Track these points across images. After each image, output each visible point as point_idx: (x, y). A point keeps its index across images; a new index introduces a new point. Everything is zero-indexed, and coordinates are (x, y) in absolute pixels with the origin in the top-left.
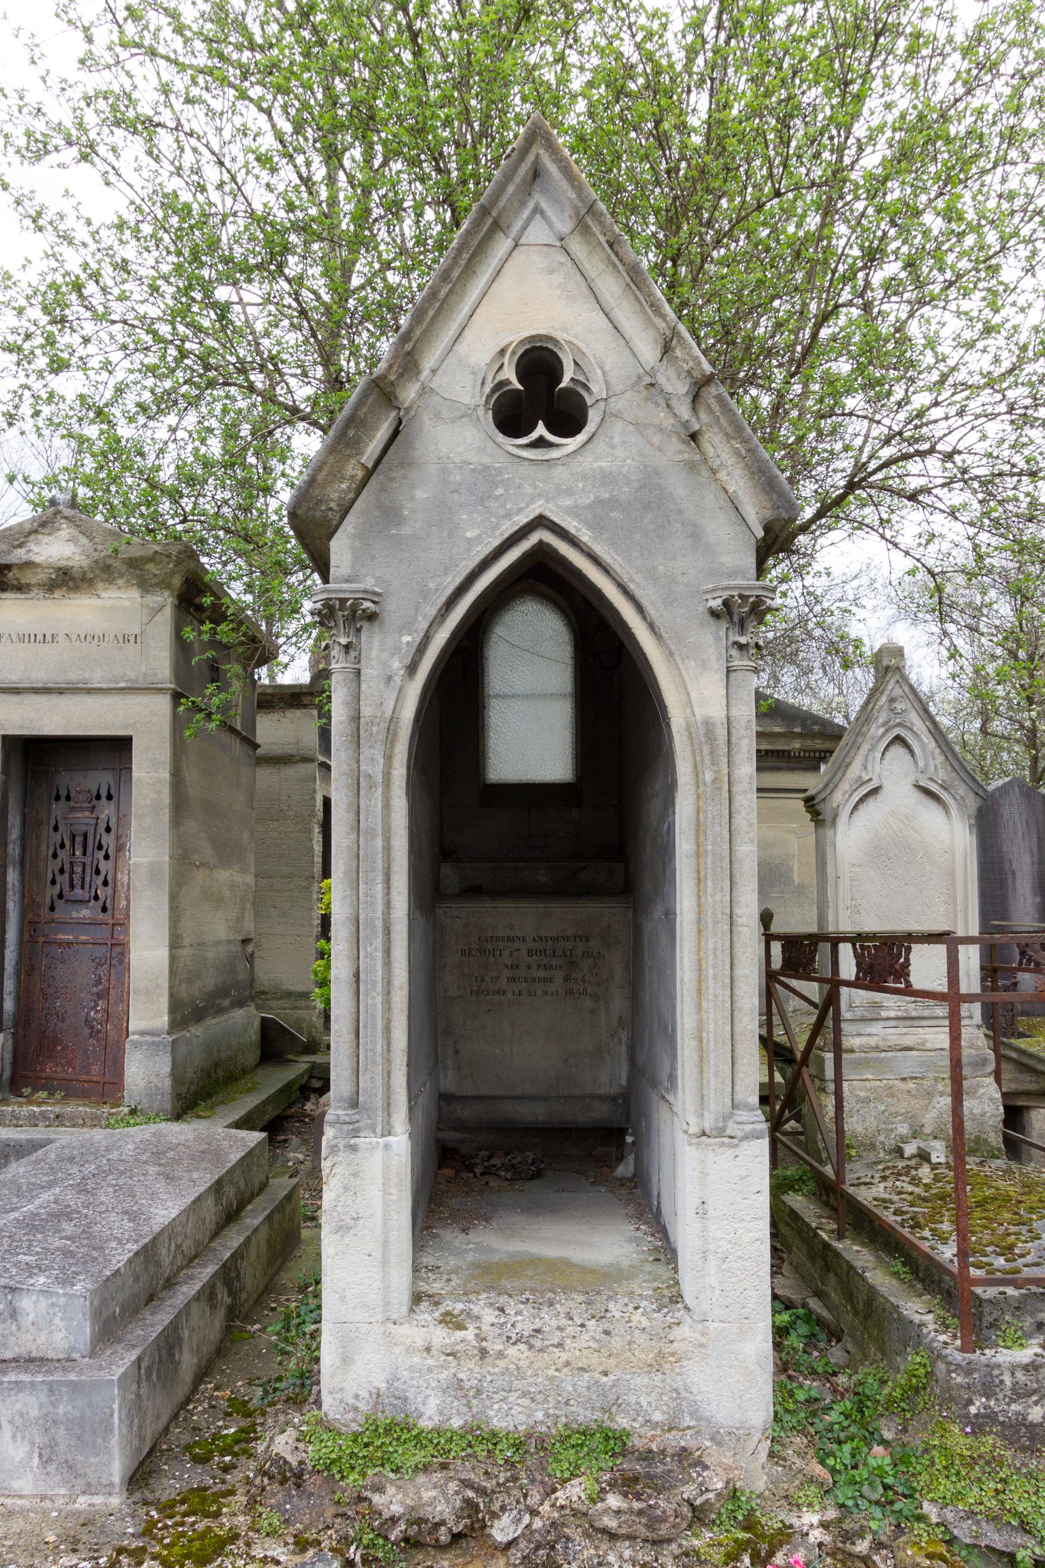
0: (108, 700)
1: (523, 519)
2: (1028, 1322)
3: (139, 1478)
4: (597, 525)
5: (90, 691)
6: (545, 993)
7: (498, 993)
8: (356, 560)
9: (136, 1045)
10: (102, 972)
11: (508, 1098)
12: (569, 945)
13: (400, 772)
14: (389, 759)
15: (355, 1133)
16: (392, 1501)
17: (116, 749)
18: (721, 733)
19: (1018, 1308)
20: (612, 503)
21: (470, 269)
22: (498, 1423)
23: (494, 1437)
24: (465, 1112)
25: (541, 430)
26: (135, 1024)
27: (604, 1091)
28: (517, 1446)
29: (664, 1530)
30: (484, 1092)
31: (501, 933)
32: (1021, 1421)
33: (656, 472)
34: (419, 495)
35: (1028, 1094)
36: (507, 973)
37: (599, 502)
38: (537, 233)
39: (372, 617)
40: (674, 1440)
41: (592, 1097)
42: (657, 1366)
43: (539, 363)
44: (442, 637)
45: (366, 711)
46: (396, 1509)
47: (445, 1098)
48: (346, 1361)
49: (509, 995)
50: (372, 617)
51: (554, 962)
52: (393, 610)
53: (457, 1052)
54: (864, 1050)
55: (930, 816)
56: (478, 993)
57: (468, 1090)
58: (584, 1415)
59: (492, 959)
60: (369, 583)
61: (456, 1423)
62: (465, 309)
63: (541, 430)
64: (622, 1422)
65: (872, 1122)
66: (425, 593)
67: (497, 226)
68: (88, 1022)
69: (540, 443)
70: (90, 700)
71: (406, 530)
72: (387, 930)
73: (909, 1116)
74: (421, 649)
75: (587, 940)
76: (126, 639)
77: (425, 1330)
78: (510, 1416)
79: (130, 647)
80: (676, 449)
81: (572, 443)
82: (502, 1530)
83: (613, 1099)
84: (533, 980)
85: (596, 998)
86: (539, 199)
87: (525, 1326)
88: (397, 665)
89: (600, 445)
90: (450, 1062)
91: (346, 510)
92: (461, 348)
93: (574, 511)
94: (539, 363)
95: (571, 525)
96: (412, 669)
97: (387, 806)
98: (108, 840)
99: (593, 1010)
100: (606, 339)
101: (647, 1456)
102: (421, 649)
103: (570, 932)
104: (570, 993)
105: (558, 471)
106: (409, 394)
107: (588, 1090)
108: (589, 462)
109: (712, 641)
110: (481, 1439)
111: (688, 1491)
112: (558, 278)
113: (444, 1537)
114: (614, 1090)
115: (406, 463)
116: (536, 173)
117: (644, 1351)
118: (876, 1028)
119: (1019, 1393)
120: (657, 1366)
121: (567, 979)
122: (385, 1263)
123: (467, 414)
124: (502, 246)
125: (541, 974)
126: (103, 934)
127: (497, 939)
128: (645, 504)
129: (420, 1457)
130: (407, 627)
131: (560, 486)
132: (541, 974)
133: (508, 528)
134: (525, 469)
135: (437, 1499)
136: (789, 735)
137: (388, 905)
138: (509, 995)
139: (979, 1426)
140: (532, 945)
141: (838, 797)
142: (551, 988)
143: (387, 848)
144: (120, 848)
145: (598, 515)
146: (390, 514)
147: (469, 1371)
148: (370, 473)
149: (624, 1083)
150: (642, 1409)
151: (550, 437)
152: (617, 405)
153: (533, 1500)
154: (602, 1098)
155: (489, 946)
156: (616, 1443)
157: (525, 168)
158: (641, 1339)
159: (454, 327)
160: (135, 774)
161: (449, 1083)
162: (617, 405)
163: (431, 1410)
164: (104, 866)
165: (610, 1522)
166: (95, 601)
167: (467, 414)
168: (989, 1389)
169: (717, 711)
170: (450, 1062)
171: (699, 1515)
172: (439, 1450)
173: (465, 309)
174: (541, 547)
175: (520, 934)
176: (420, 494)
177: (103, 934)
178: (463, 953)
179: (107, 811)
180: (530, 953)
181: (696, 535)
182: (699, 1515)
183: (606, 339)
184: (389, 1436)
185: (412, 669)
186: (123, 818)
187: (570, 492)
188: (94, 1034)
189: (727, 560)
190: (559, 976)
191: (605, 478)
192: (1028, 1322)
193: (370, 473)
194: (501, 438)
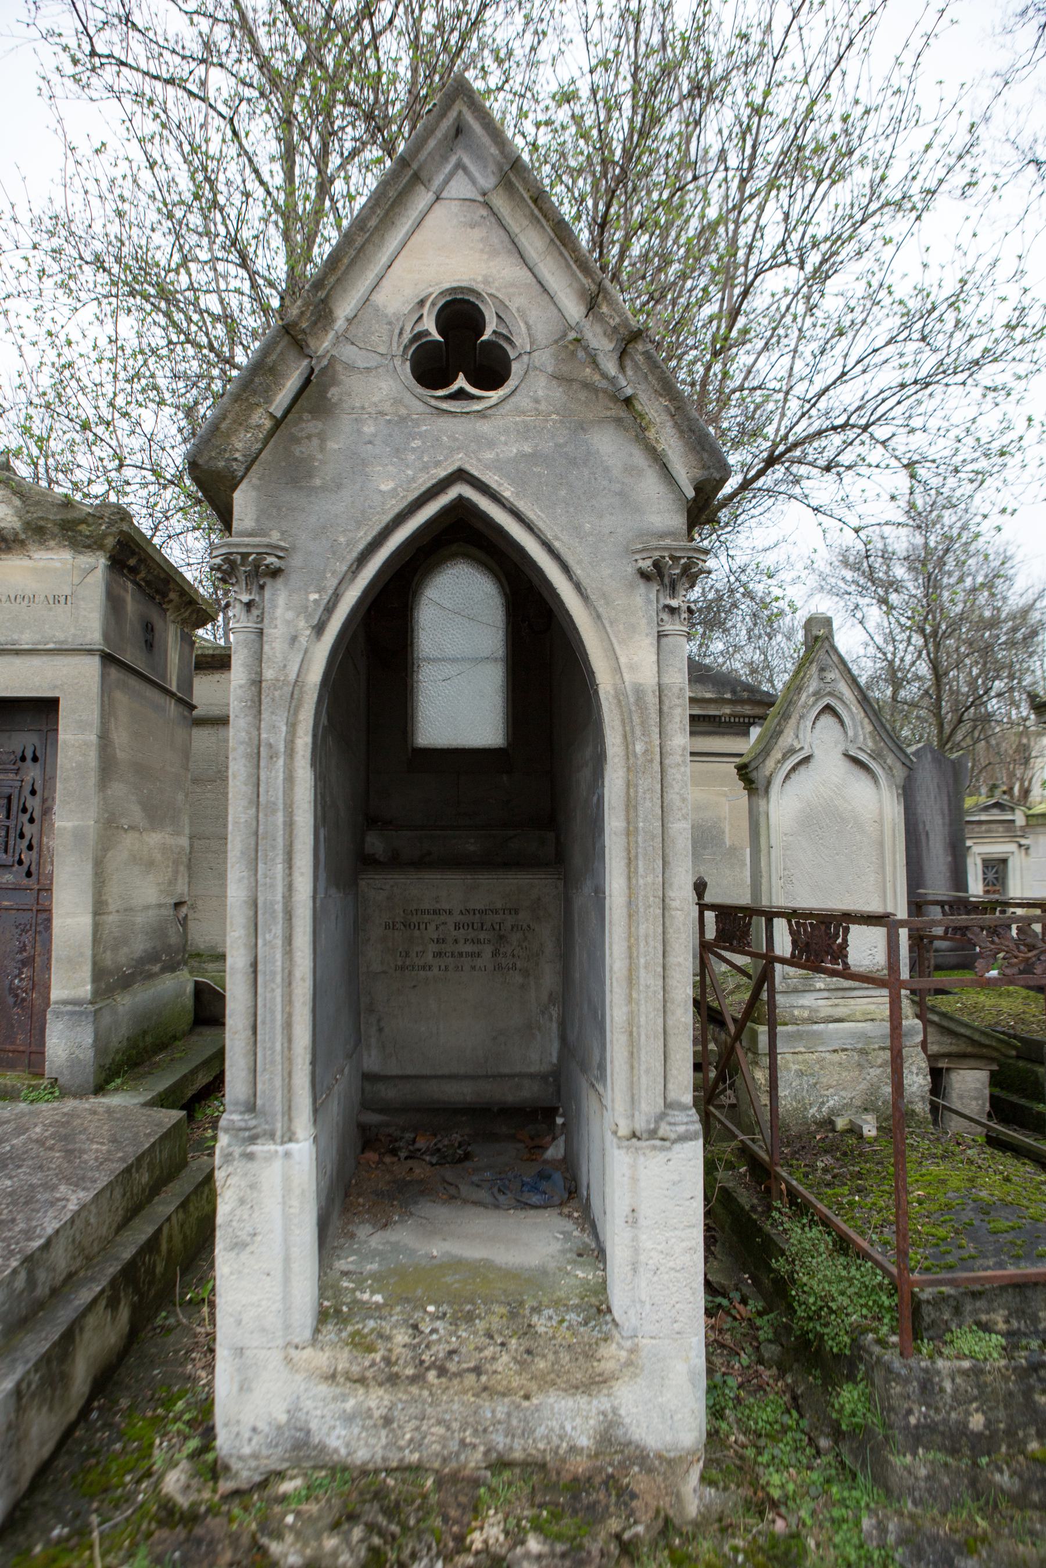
1: (442, 473)
6: (473, 968)
7: (424, 968)
8: (263, 513)
11: (436, 1077)
12: (497, 918)
13: (304, 741)
14: (292, 727)
18: (652, 700)
24: (389, 1093)
25: (461, 382)
26: (56, 994)
27: (533, 1069)
30: (410, 1071)
31: (426, 906)
36: (432, 948)
38: (459, 187)
39: (275, 573)
41: (521, 1075)
43: (460, 314)
45: (269, 674)
47: (369, 1078)
49: (436, 970)
51: (482, 936)
53: (380, 1030)
56: (402, 968)
57: (393, 1069)
59: (417, 933)
60: (275, 537)
62: (383, 259)
63: (461, 382)
67: (417, 179)
69: (460, 395)
75: (516, 912)
81: (495, 395)
83: (543, 1077)
84: (461, 954)
85: (526, 973)
90: (373, 1040)
93: (497, 466)
94: (460, 314)
95: (491, 479)
97: (290, 779)
99: (522, 986)
102: (330, 609)
103: (499, 905)
104: (498, 968)
107: (517, 1069)
114: (545, 1068)
116: (459, 130)
121: (495, 953)
124: (422, 198)
125: (468, 948)
127: (423, 912)
132: (468, 948)
133: (425, 482)
137: (290, 887)
138: (436, 970)
140: (458, 918)
142: (479, 962)
143: (290, 825)
149: (555, 1060)
154: (532, 1076)
155: (415, 919)
157: (447, 123)
161: (372, 1062)
170: (373, 1040)
173: (383, 259)
174: (461, 502)
175: (446, 906)
178: (387, 926)
180: (457, 926)
185: (319, 629)
190: (488, 950)
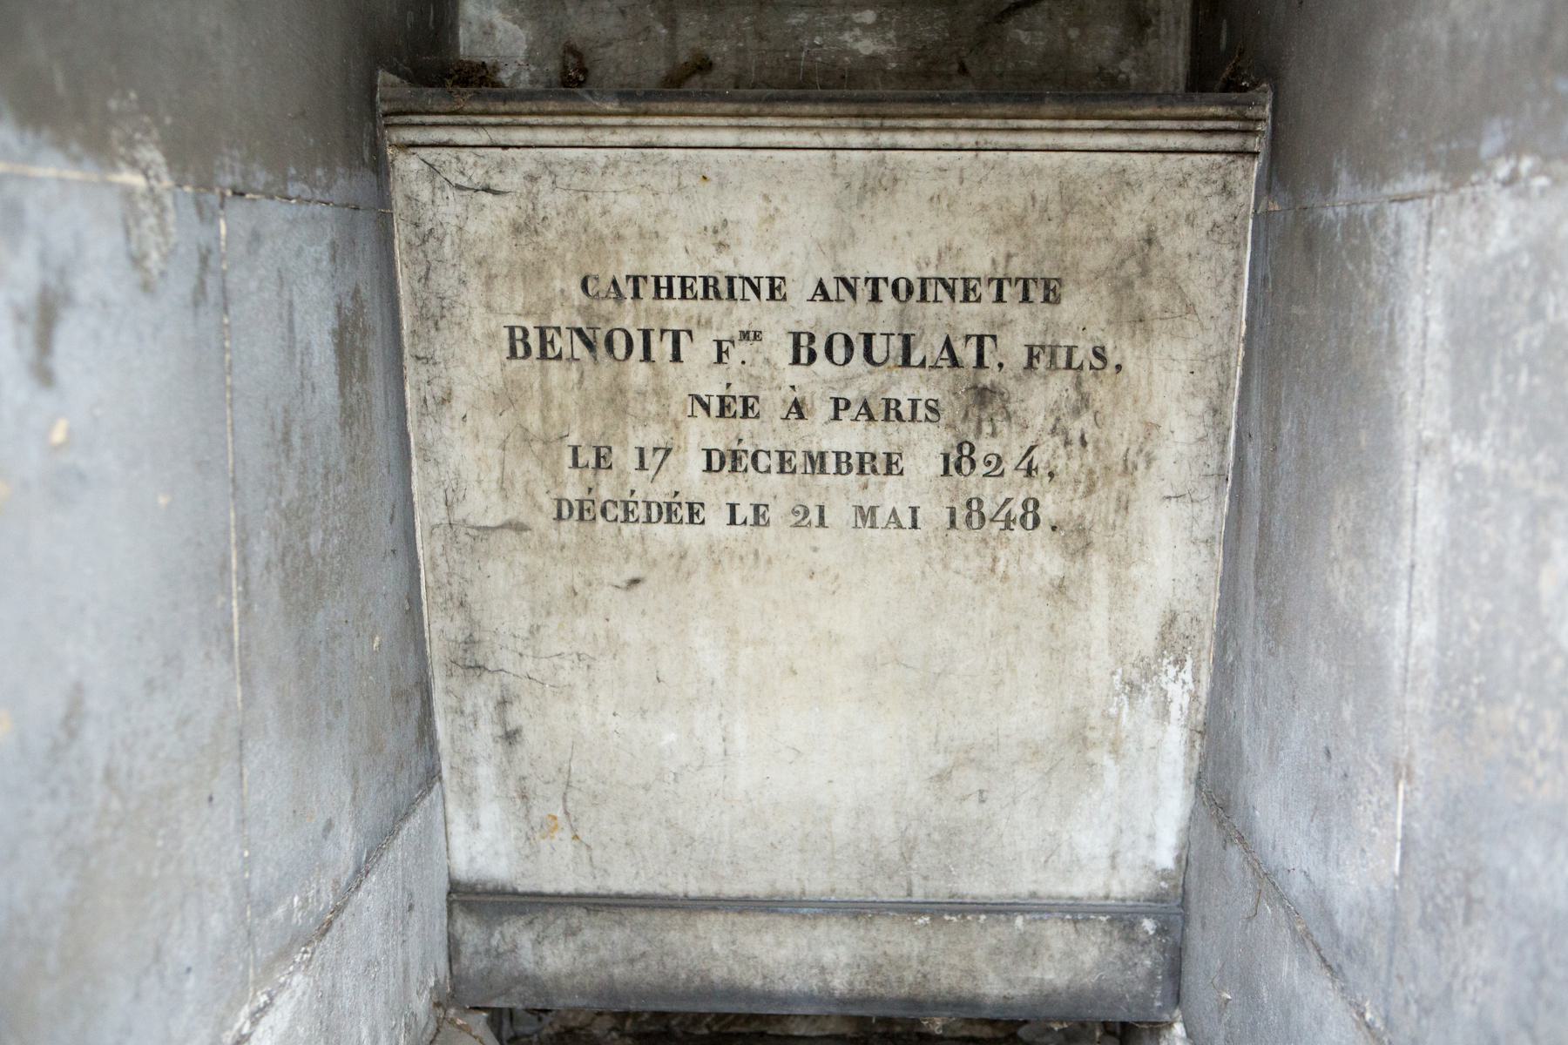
6: (866, 515)
7: (668, 512)
11: (714, 904)
12: (971, 317)
24: (552, 958)
27: (1084, 885)
30: (622, 881)
31: (674, 261)
36: (706, 432)
41: (1036, 908)
47: (472, 899)
49: (716, 519)
51: (908, 387)
53: (511, 737)
56: (582, 511)
57: (560, 871)
59: (638, 372)
75: (1052, 295)
83: (1122, 918)
84: (817, 462)
85: (1076, 539)
90: (485, 773)
99: (1061, 587)
103: (979, 261)
104: (972, 514)
107: (1022, 884)
114: (1128, 884)
121: (957, 461)
125: (850, 436)
127: (664, 288)
132: (850, 436)
138: (716, 519)
140: (806, 313)
142: (890, 494)
149: (1165, 858)
154: (1077, 912)
155: (629, 317)
161: (482, 843)
170: (485, 773)
175: (759, 268)
178: (517, 345)
180: (802, 349)
190: (925, 447)
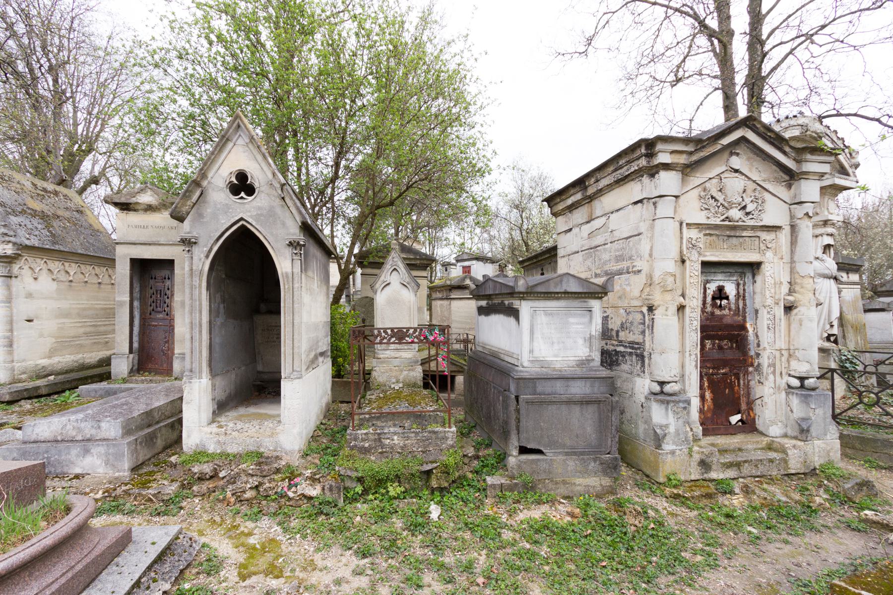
0: (166, 248)
1: (237, 218)
2: (370, 424)
3: (134, 469)
4: (257, 221)
5: (160, 245)
8: (191, 227)
9: (177, 358)
10: (167, 334)
13: (204, 284)
14: (200, 280)
15: (191, 379)
16: (196, 469)
17: (171, 263)
18: (290, 276)
19: (368, 420)
20: (261, 215)
21: (221, 151)
22: (229, 451)
23: (228, 455)
25: (243, 194)
28: (234, 456)
29: (264, 473)
32: (363, 447)
33: (273, 207)
34: (208, 211)
35: (455, 371)
37: (258, 214)
38: (240, 142)
39: (195, 243)
40: (275, 454)
42: (271, 436)
43: (242, 176)
44: (216, 248)
45: (194, 268)
46: (196, 471)
48: (189, 436)
50: (195, 243)
52: (201, 241)
54: (384, 358)
55: (404, 291)
58: (252, 448)
60: (195, 234)
61: (218, 451)
62: (220, 161)
63: (243, 194)
64: (262, 450)
65: (385, 379)
66: (210, 237)
67: (228, 140)
68: (162, 351)
69: (242, 198)
70: (160, 247)
71: (205, 220)
72: (201, 325)
73: (396, 377)
74: (210, 251)
76: (172, 228)
77: (214, 428)
78: (232, 449)
79: (173, 231)
80: (278, 202)
81: (250, 198)
82: (221, 475)
86: (240, 132)
87: (239, 427)
88: (203, 256)
89: (258, 199)
91: (188, 214)
92: (220, 171)
93: (251, 217)
94: (242, 176)
95: (250, 220)
96: (207, 257)
97: (200, 293)
98: (168, 292)
100: (260, 172)
101: (268, 458)
102: (210, 251)
105: (247, 206)
106: (205, 183)
108: (255, 204)
109: (288, 252)
110: (224, 455)
111: (276, 465)
112: (246, 154)
113: (208, 477)
115: (204, 202)
116: (239, 126)
117: (268, 433)
118: (388, 352)
119: (363, 440)
120: (271, 436)
122: (199, 412)
123: (221, 189)
124: (230, 145)
126: (167, 322)
128: (270, 215)
129: (206, 459)
130: (206, 246)
131: (247, 211)
133: (233, 221)
134: (237, 205)
135: (207, 468)
136: (415, 259)
137: (201, 319)
139: (352, 448)
141: (377, 286)
143: (200, 304)
144: (173, 295)
145: (257, 217)
146: (200, 216)
147: (222, 438)
148: (195, 204)
150: (267, 447)
151: (245, 196)
152: (262, 189)
153: (234, 467)
156: (260, 455)
157: (235, 125)
158: (268, 429)
159: (217, 166)
160: (176, 272)
162: (262, 189)
163: (212, 448)
164: (167, 301)
165: (251, 472)
166: (161, 215)
167: (221, 189)
168: (355, 440)
169: (289, 270)
171: (278, 471)
172: (211, 457)
173: (220, 161)
174: (243, 226)
176: (209, 210)
177: (167, 322)
179: (168, 283)
181: (284, 224)
182: (278, 471)
183: (260, 172)
184: (200, 455)
185: (207, 257)
186: (173, 285)
187: (250, 211)
188: (164, 354)
189: (292, 231)
191: (259, 208)
192: (370, 424)
193: (195, 204)
194: (231, 196)
